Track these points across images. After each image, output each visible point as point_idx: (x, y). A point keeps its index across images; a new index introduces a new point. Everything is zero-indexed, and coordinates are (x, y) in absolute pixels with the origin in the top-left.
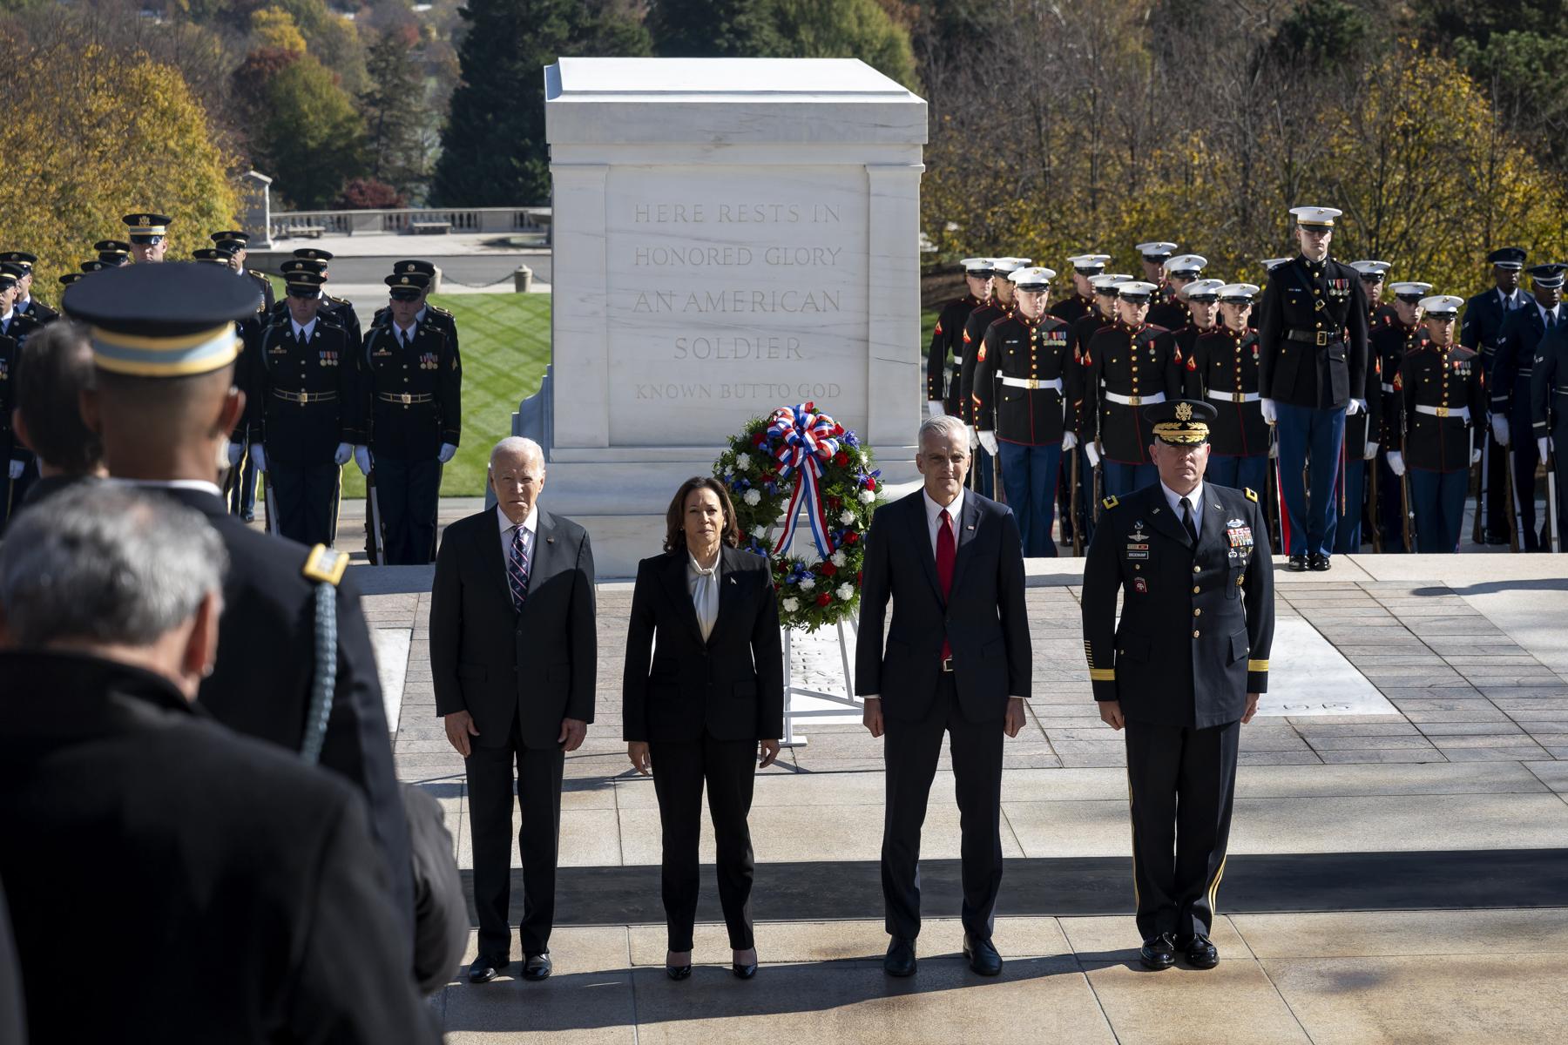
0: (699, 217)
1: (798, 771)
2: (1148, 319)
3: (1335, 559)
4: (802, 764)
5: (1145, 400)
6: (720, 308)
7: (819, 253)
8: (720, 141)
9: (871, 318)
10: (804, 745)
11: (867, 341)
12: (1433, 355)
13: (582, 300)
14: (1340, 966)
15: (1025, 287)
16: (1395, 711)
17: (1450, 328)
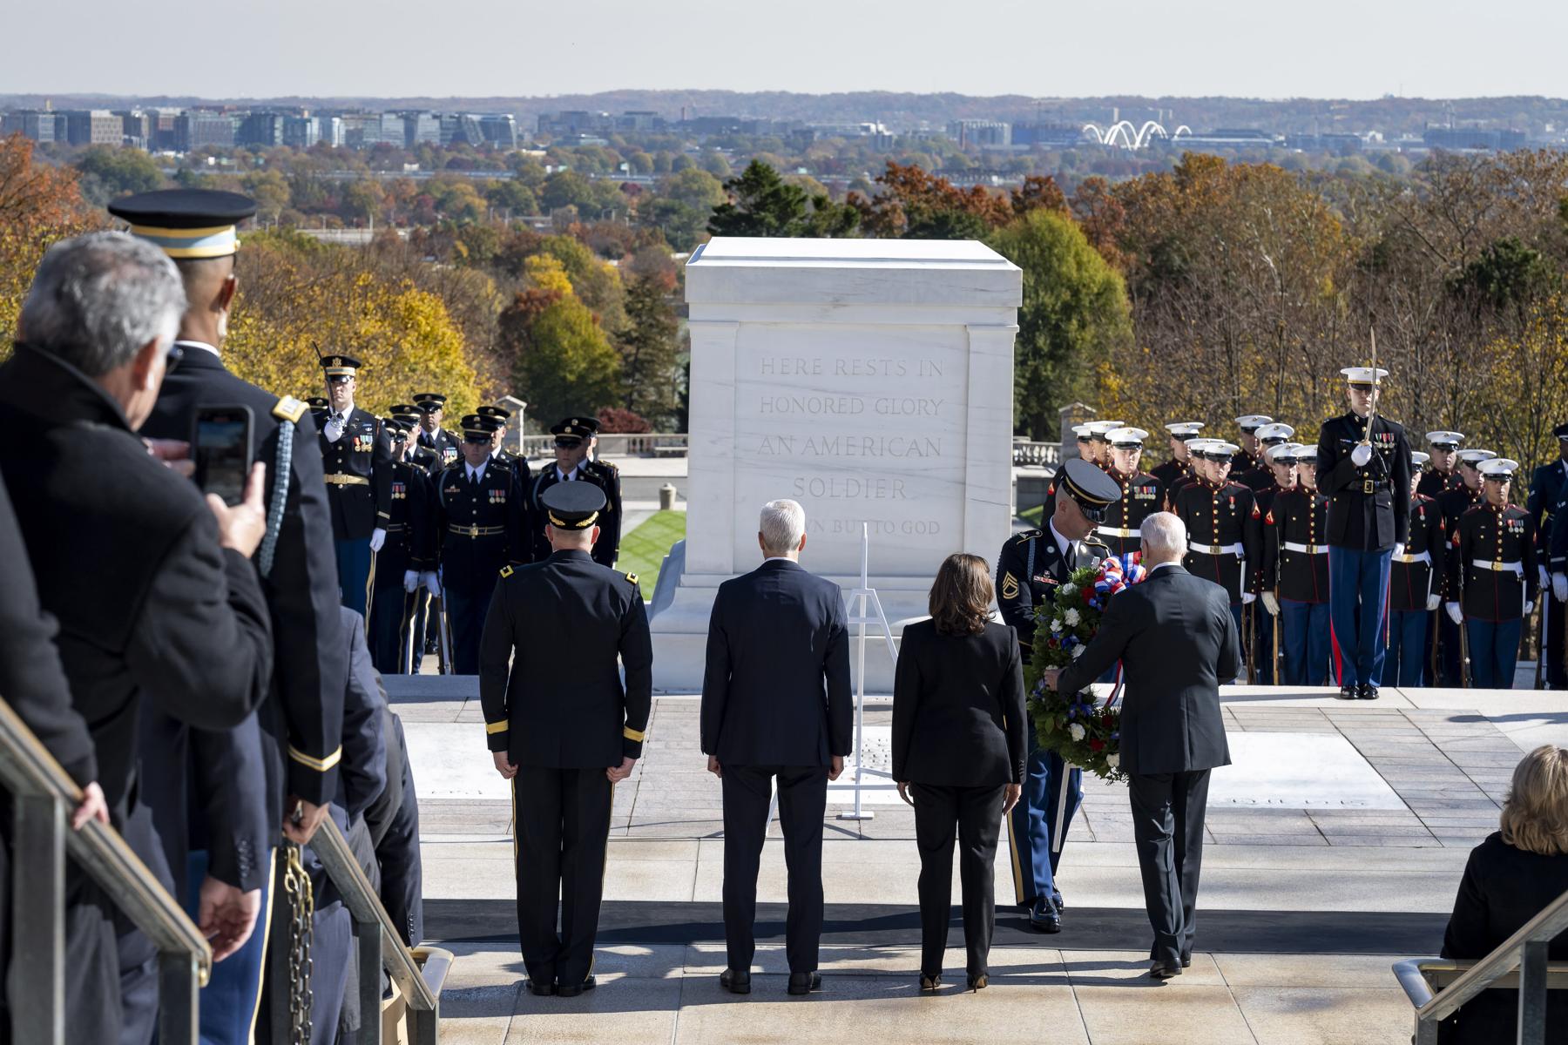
0: (818, 370)
1: (861, 838)
2: (1230, 476)
3: (1384, 692)
4: (865, 833)
5: (1225, 550)
6: (834, 451)
7: (923, 404)
8: (837, 302)
9: (969, 463)
10: (870, 819)
11: (964, 483)
12: (1488, 513)
13: (713, 442)
14: (1301, 993)
15: (1121, 445)
16: (1405, 807)
17: (1505, 489)
